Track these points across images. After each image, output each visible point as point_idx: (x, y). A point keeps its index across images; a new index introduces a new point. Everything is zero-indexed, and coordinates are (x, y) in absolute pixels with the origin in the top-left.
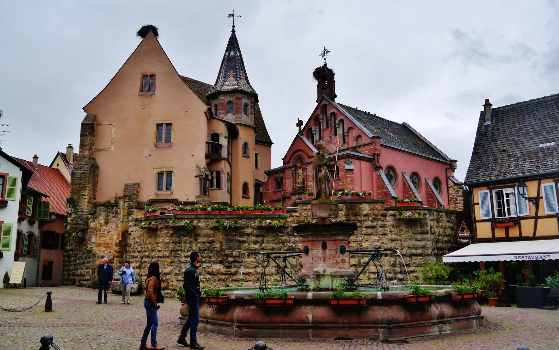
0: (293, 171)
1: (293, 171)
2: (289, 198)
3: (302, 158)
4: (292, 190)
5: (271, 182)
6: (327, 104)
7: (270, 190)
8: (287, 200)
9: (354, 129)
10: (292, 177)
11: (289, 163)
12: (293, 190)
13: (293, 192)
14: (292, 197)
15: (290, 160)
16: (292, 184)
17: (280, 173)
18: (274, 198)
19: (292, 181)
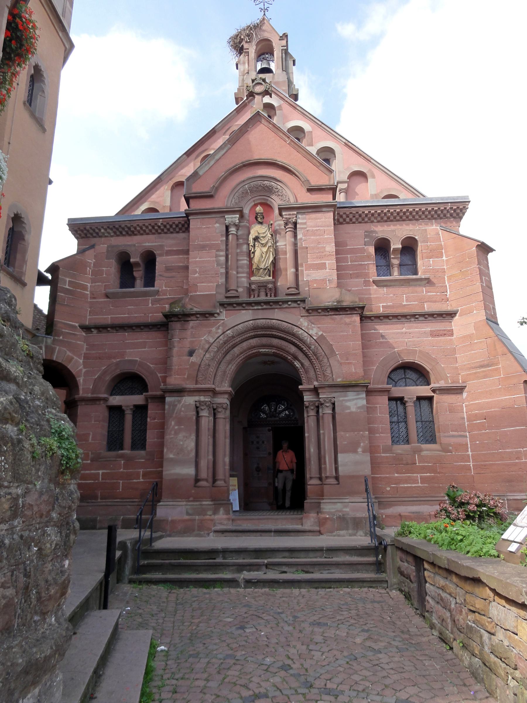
0: (227, 228)
1: (227, 228)
2: (207, 315)
3: (269, 190)
4: (223, 290)
5: (91, 261)
6: (276, 104)
7: (85, 288)
8: (191, 323)
9: (373, 177)
10: (224, 247)
11: (211, 197)
12: (227, 291)
13: (227, 297)
14: (223, 316)
15: (217, 189)
16: (223, 271)
17: (151, 233)
18: (107, 319)
19: (223, 259)
